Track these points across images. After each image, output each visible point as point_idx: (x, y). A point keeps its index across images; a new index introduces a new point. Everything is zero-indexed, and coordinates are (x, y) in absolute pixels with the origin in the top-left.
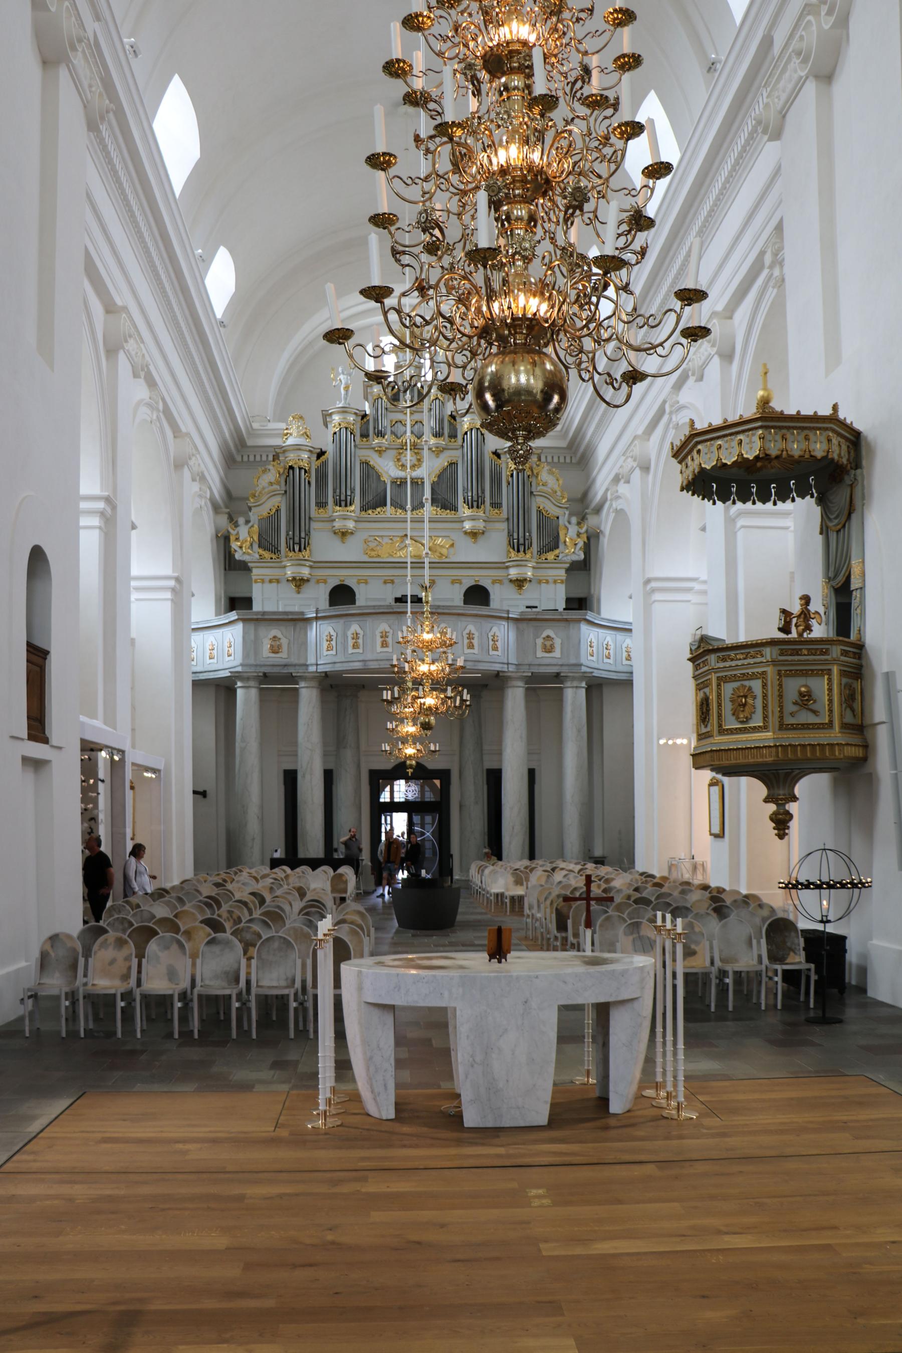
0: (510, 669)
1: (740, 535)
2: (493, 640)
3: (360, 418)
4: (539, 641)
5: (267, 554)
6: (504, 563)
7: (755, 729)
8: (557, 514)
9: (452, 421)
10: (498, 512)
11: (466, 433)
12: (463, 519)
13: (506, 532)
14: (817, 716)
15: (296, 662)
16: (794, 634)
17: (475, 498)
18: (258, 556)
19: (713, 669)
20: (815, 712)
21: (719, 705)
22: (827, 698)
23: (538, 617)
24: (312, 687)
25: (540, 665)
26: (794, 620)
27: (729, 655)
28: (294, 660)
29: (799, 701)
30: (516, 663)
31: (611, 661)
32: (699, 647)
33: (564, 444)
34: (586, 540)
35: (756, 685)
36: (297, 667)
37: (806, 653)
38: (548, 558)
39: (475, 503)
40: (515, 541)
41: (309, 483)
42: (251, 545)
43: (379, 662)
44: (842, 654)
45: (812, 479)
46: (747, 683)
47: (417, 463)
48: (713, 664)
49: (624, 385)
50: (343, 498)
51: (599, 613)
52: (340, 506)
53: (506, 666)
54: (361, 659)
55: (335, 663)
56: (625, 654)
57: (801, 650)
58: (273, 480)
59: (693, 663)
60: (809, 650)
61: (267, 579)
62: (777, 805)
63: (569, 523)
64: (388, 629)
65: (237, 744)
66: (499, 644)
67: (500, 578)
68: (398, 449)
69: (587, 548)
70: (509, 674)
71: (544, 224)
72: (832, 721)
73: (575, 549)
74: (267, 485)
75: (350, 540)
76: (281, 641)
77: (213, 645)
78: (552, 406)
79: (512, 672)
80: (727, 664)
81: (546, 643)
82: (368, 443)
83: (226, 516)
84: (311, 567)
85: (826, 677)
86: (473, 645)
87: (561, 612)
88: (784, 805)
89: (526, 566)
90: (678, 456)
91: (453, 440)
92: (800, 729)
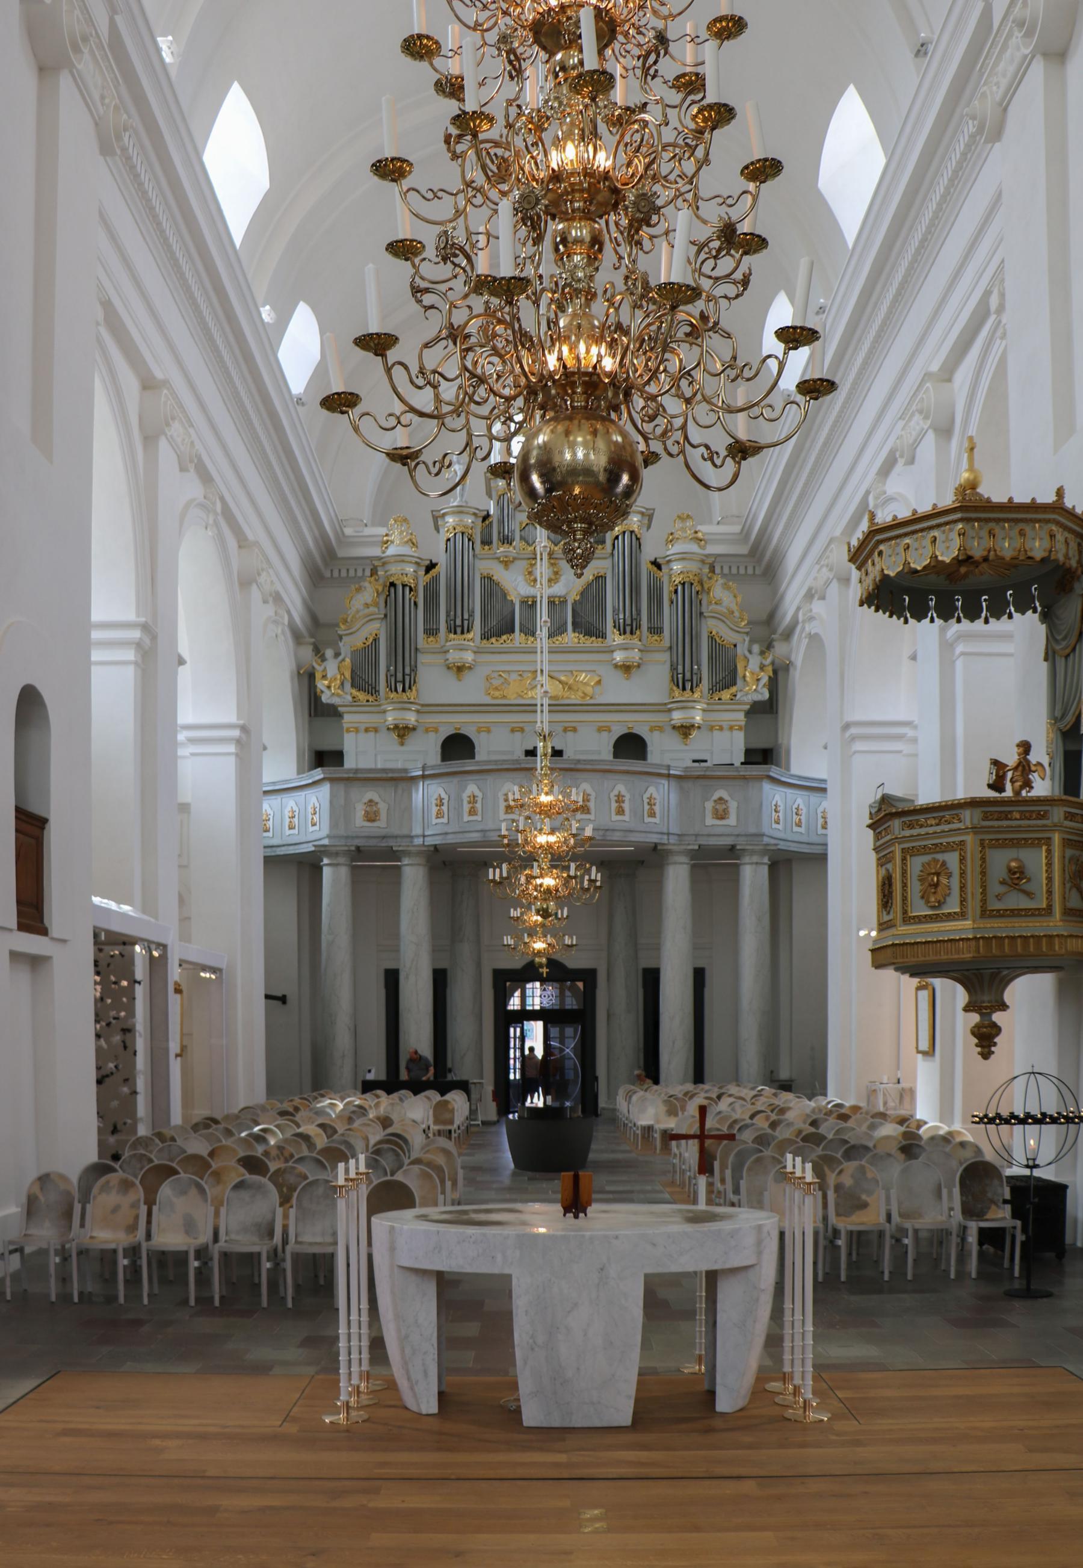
0: (671, 841)
1: (959, 664)
2: (649, 804)
3: (481, 519)
4: (709, 805)
5: (362, 696)
6: (665, 704)
7: (950, 917)
8: (734, 642)
10: (658, 639)
11: (617, 538)
12: (612, 648)
14: (1032, 899)
15: (397, 832)
16: (1009, 792)
17: (628, 622)
18: (349, 698)
19: (896, 838)
20: (1029, 894)
21: (904, 885)
22: (1044, 875)
23: (708, 773)
24: (419, 865)
25: (709, 835)
26: (1010, 775)
27: (918, 820)
29: (1007, 879)
30: (680, 833)
31: (802, 830)
32: (879, 810)
33: (744, 550)
34: (771, 674)
35: (952, 859)
36: (399, 840)
37: (1018, 816)
38: (723, 697)
39: (629, 628)
40: (680, 676)
41: (416, 604)
42: (342, 684)
44: (1066, 818)
45: (1035, 589)
46: (940, 857)
47: (553, 577)
48: (897, 832)
49: (729, 460)
50: (458, 622)
51: (788, 768)
52: (455, 633)
53: (666, 837)
54: (479, 827)
55: (446, 834)
56: (821, 821)
57: (1011, 812)
58: (369, 601)
59: (874, 830)
60: (1021, 812)
61: (363, 727)
62: (981, 1014)
63: (750, 652)
65: (323, 937)
66: (657, 808)
67: (660, 724)
68: (529, 559)
69: (773, 685)
70: (669, 847)
71: (617, 248)
72: (1051, 906)
73: (757, 686)
75: (468, 676)
76: (379, 806)
77: (293, 812)
78: (620, 489)
79: (674, 845)
80: (915, 832)
81: (717, 807)
82: (491, 552)
83: (311, 648)
84: (418, 711)
85: (1044, 848)
86: (623, 811)
87: (737, 768)
88: (990, 1014)
89: (693, 708)
90: (857, 560)
92: (1009, 916)
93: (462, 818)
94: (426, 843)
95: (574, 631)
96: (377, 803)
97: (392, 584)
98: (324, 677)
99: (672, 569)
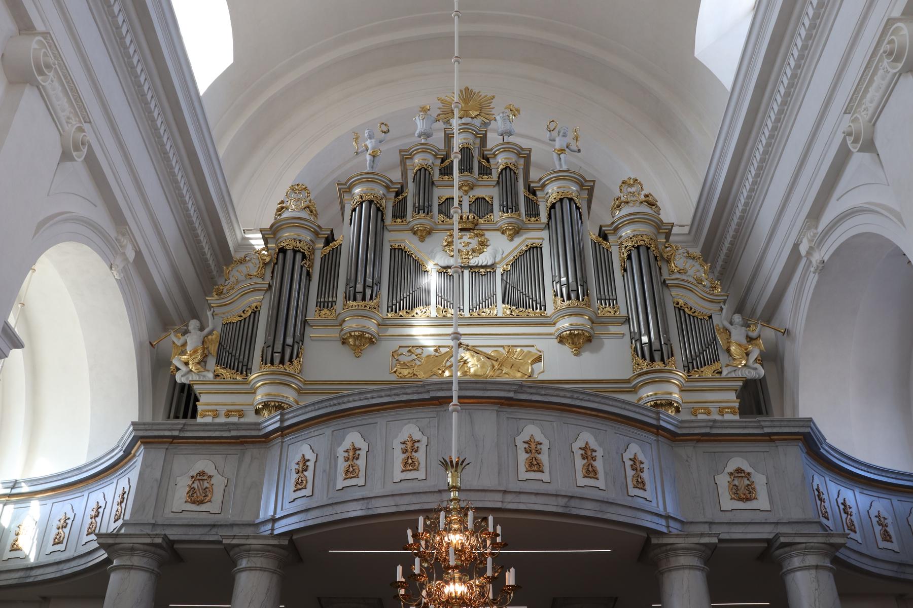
4: (723, 480)
8: (709, 313)
9: (531, 197)
11: (553, 206)
18: (210, 376)
23: (715, 431)
24: (261, 569)
28: (230, 516)
41: (309, 274)
43: (397, 498)
50: (359, 288)
52: (355, 300)
54: (359, 494)
64: (417, 436)
73: (747, 361)
74: (243, 278)
76: (213, 481)
84: (300, 392)
86: (595, 472)
91: (533, 219)
93: (335, 485)
94: (276, 532)
95: (504, 302)
96: (210, 477)
98: (183, 353)
99: (621, 237)
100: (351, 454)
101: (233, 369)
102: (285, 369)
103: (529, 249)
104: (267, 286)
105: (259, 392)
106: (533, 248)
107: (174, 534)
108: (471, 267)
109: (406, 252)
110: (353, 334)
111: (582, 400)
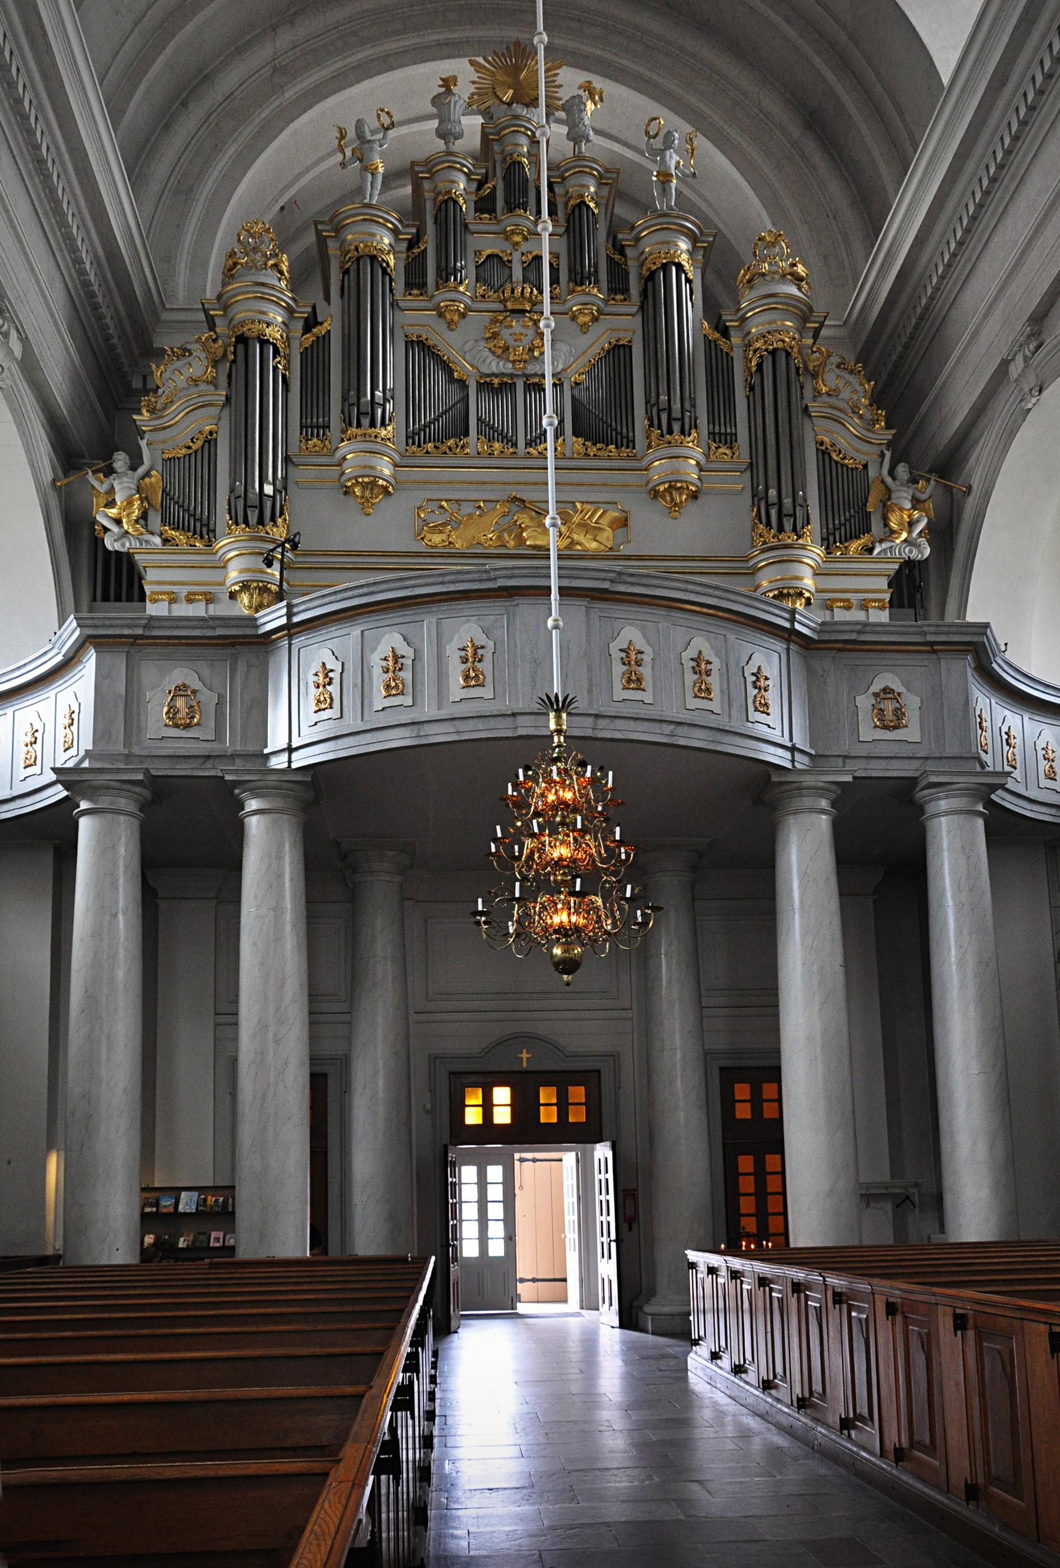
9: (617, 257)
10: (728, 452)
13: (748, 493)
18: (157, 540)
42: (144, 516)
43: (457, 723)
52: (359, 425)
54: (405, 718)
61: (183, 591)
64: (481, 639)
76: (200, 697)
86: (708, 690)
91: (619, 297)
93: (371, 703)
94: (294, 766)
95: (575, 434)
96: (194, 692)
97: (242, 340)
98: (111, 504)
100: (391, 663)
101: (189, 530)
102: (267, 533)
103: (613, 348)
104: (224, 398)
105: (231, 565)
106: (619, 346)
107: (160, 769)
108: (528, 377)
109: (429, 347)
110: (360, 480)
111: (698, 593)
